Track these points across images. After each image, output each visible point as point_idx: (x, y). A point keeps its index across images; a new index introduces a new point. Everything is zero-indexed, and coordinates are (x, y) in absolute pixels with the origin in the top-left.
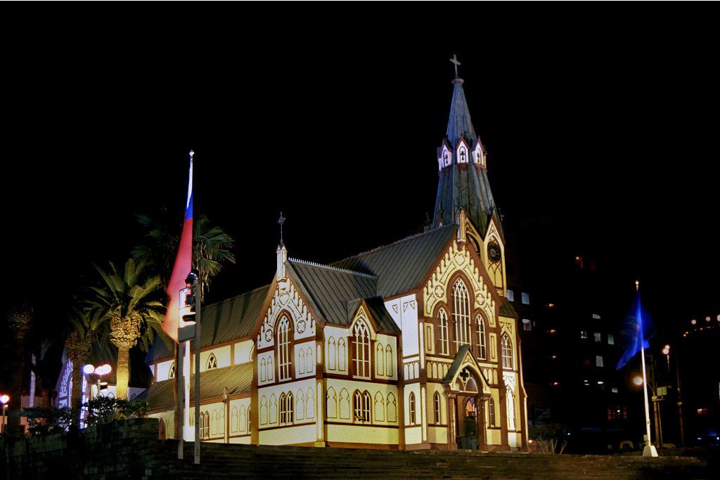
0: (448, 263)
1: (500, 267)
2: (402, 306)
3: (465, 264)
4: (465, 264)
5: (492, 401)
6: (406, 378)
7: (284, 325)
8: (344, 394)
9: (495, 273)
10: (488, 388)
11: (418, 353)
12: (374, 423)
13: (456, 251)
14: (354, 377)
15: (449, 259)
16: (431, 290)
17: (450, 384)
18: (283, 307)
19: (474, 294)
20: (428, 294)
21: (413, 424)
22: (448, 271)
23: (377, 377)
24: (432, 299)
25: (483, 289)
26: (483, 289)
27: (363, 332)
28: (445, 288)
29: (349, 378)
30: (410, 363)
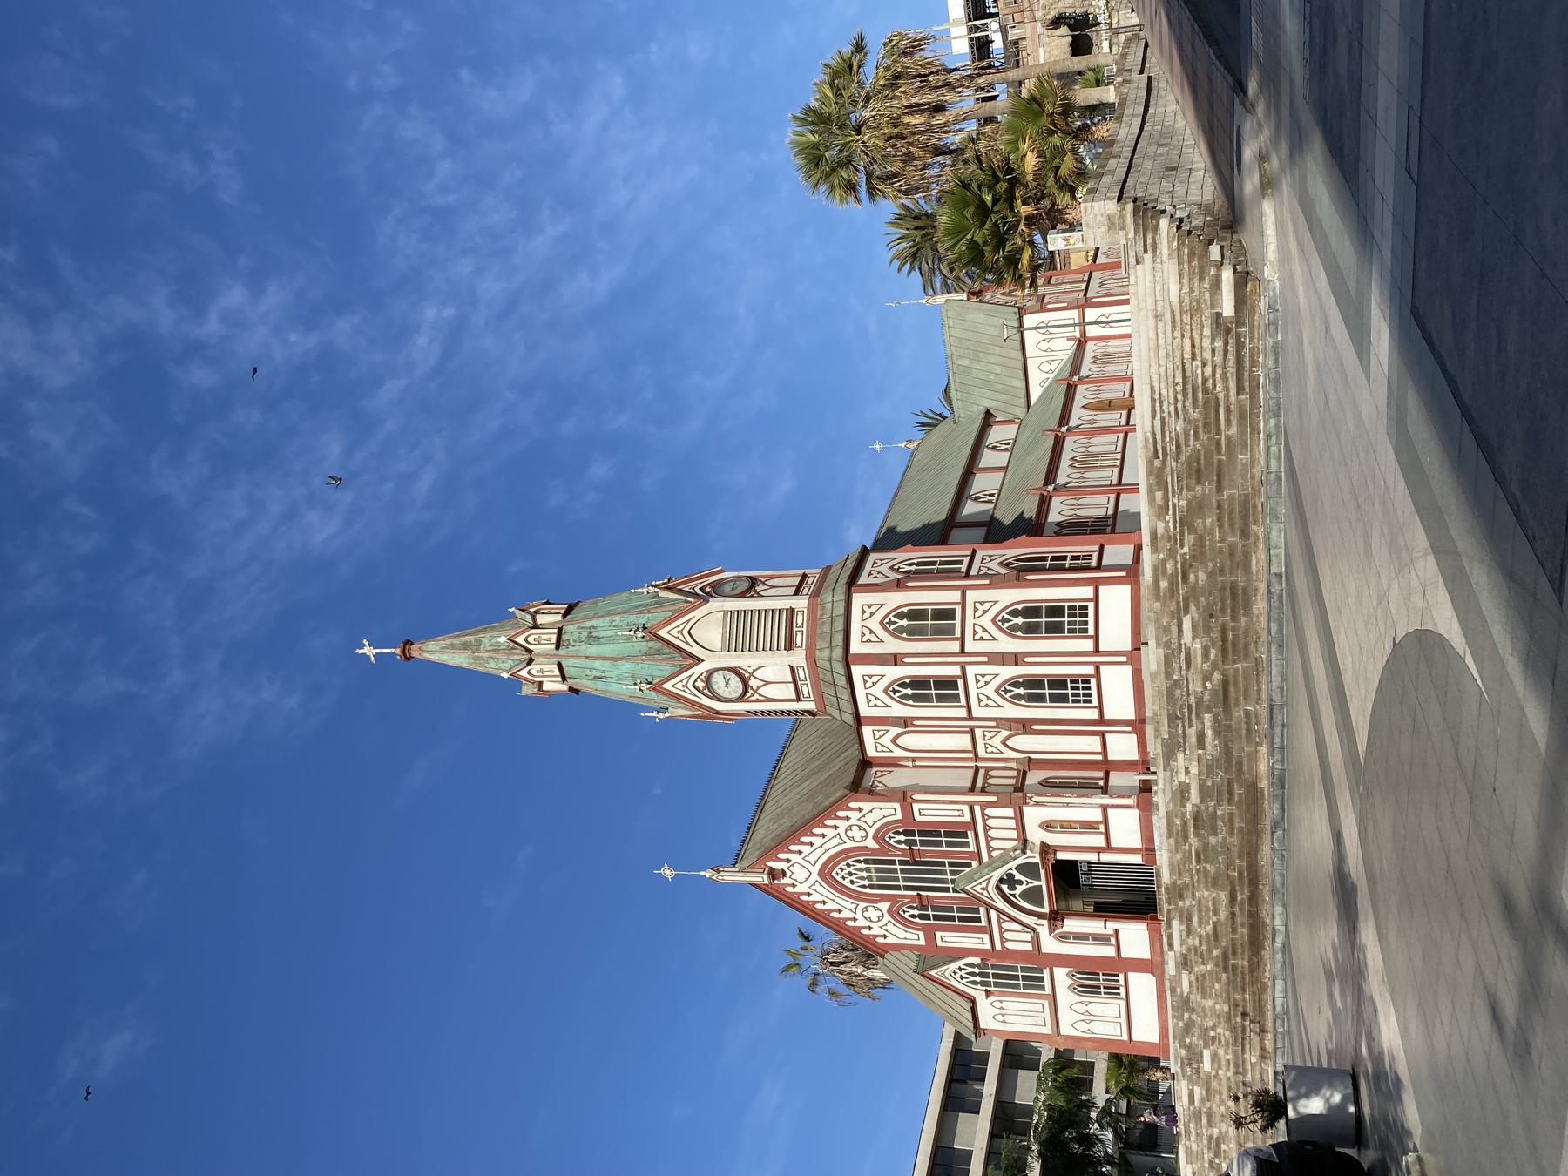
5: (1048, 826)
8: (1080, 1008)
9: (767, 683)
13: (786, 881)
16: (876, 931)
21: (1113, 941)
22: (832, 897)
25: (836, 827)
26: (836, 827)
27: (971, 970)
28: (862, 905)
29: (1053, 998)
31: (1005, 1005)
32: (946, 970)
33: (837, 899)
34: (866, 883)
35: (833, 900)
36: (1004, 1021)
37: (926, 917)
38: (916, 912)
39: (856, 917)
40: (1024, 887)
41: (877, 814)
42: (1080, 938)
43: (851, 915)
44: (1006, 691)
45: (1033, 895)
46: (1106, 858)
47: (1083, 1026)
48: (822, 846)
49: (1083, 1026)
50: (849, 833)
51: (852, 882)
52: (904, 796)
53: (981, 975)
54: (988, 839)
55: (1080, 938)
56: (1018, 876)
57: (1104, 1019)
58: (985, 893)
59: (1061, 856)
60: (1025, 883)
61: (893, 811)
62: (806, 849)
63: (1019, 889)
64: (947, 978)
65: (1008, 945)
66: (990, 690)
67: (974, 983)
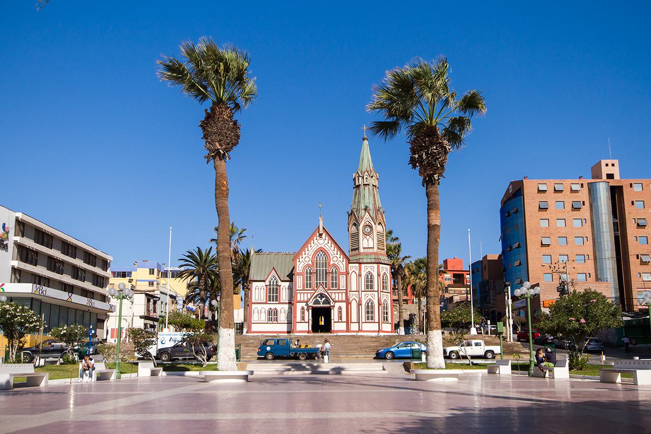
0: (312, 245)
1: (372, 237)
3: (325, 243)
4: (325, 243)
5: (340, 308)
8: (263, 310)
12: (279, 322)
13: (318, 238)
16: (301, 260)
23: (281, 301)
24: (302, 264)
27: (275, 282)
28: (311, 257)
29: (266, 303)
31: (262, 290)
33: (312, 250)
34: (318, 259)
37: (307, 273)
38: (308, 271)
40: (320, 300)
41: (342, 266)
42: (303, 313)
43: (307, 253)
44: (370, 301)
45: (317, 302)
46: (332, 321)
47: (256, 310)
49: (256, 310)
50: (335, 257)
51: (318, 255)
52: (347, 273)
53: (273, 285)
54: (335, 293)
55: (303, 313)
56: (323, 299)
57: (259, 317)
59: (332, 310)
61: (343, 270)
62: (329, 245)
63: (319, 299)
65: (299, 295)
66: (370, 297)
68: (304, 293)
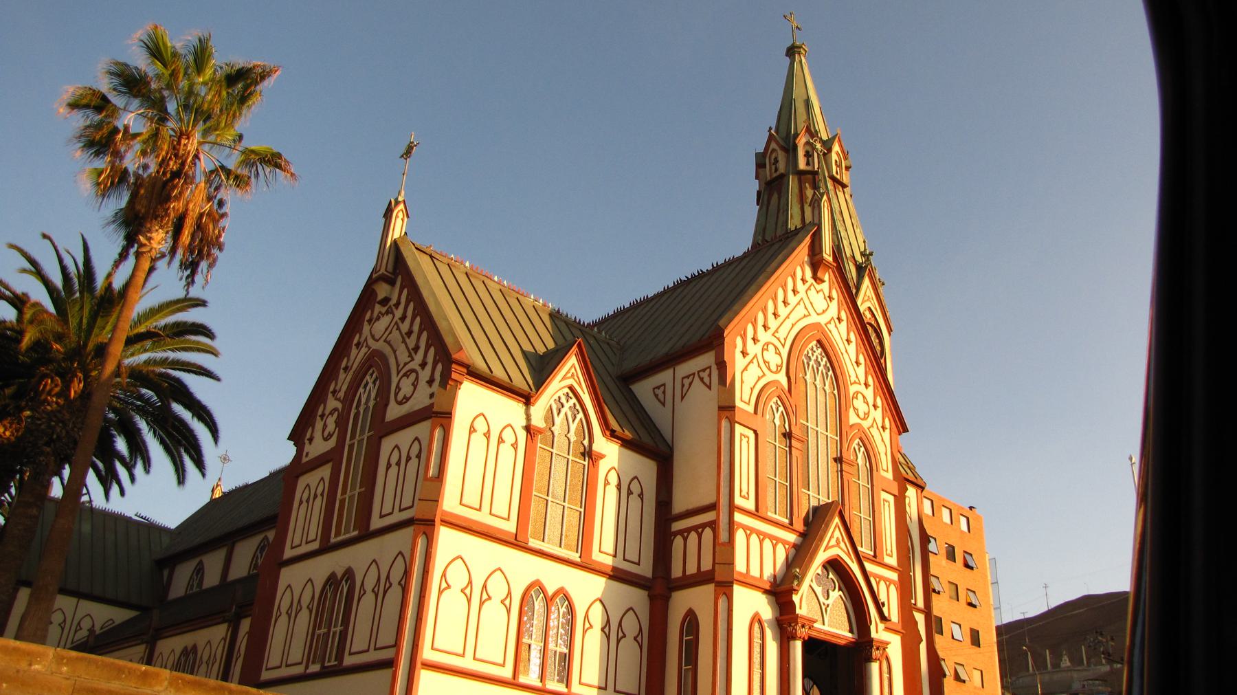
0: (792, 300)
2: (678, 386)
6: (677, 572)
7: (368, 393)
8: (497, 588)
10: (881, 626)
11: (710, 499)
14: (534, 543)
15: (795, 292)
16: (752, 349)
17: (796, 598)
18: (374, 345)
19: (846, 389)
20: (744, 354)
24: (754, 371)
28: (785, 353)
29: (516, 542)
30: (689, 530)
31: (506, 449)
32: (580, 384)
33: (788, 324)
35: (788, 317)
36: (472, 430)
39: (770, 332)
48: (846, 351)
57: (471, 629)
58: (833, 542)
60: (826, 602)
64: (564, 378)
65: (740, 536)
67: (550, 419)
68: (762, 536)
